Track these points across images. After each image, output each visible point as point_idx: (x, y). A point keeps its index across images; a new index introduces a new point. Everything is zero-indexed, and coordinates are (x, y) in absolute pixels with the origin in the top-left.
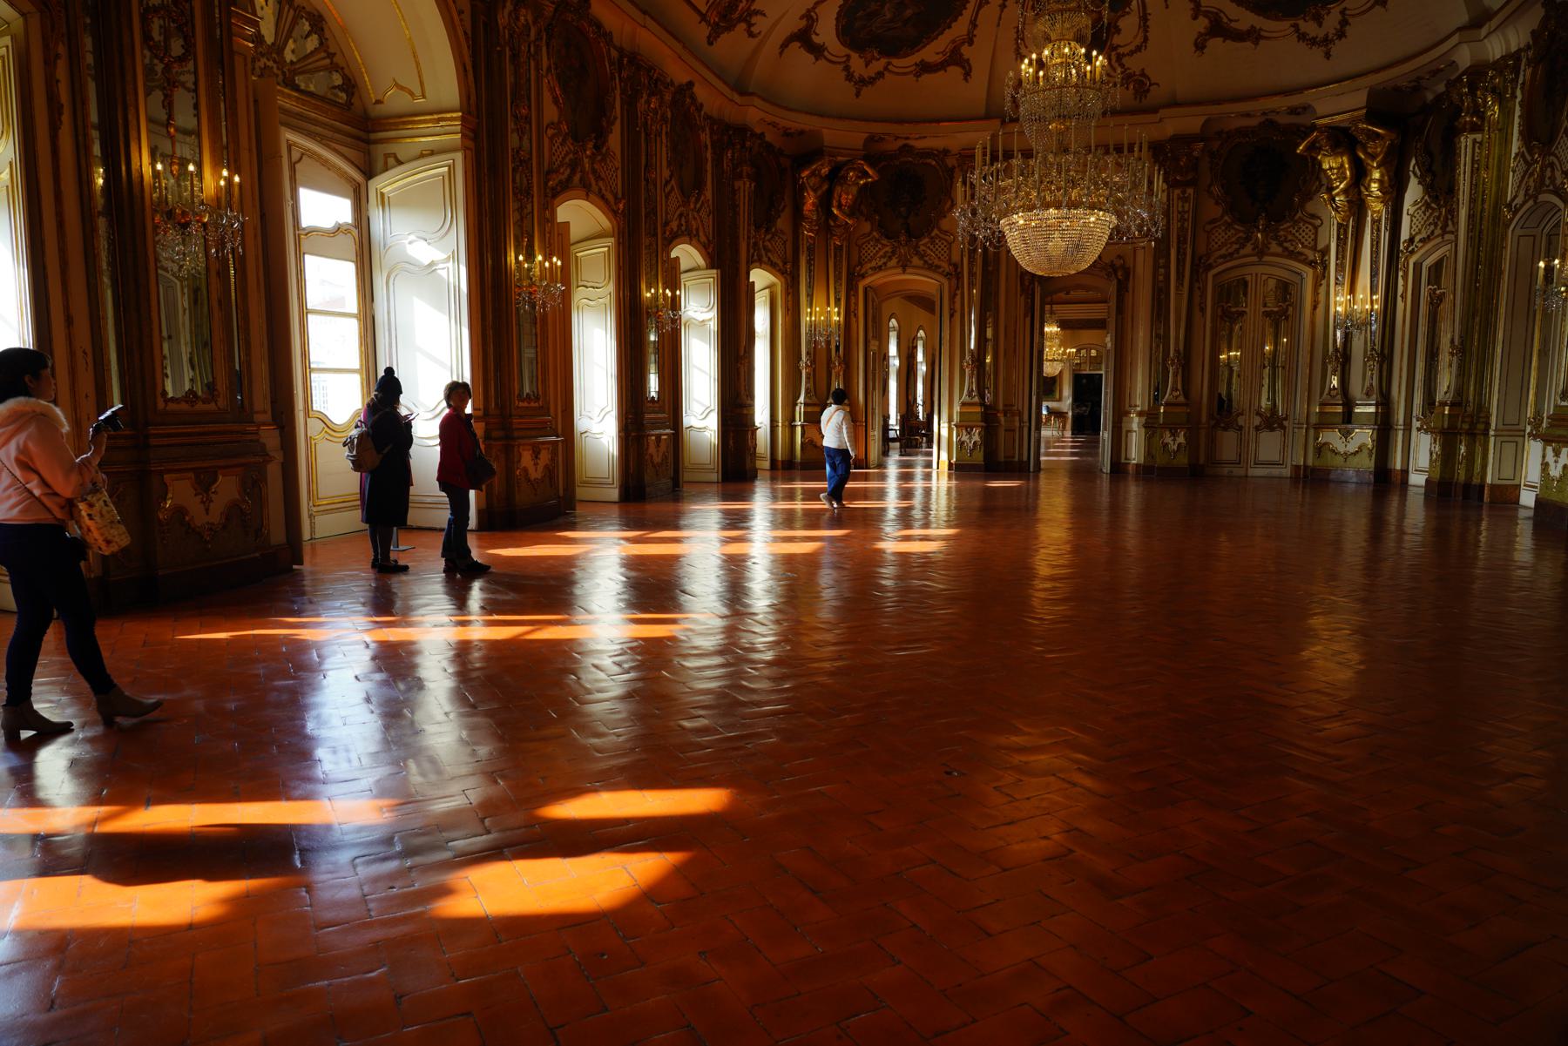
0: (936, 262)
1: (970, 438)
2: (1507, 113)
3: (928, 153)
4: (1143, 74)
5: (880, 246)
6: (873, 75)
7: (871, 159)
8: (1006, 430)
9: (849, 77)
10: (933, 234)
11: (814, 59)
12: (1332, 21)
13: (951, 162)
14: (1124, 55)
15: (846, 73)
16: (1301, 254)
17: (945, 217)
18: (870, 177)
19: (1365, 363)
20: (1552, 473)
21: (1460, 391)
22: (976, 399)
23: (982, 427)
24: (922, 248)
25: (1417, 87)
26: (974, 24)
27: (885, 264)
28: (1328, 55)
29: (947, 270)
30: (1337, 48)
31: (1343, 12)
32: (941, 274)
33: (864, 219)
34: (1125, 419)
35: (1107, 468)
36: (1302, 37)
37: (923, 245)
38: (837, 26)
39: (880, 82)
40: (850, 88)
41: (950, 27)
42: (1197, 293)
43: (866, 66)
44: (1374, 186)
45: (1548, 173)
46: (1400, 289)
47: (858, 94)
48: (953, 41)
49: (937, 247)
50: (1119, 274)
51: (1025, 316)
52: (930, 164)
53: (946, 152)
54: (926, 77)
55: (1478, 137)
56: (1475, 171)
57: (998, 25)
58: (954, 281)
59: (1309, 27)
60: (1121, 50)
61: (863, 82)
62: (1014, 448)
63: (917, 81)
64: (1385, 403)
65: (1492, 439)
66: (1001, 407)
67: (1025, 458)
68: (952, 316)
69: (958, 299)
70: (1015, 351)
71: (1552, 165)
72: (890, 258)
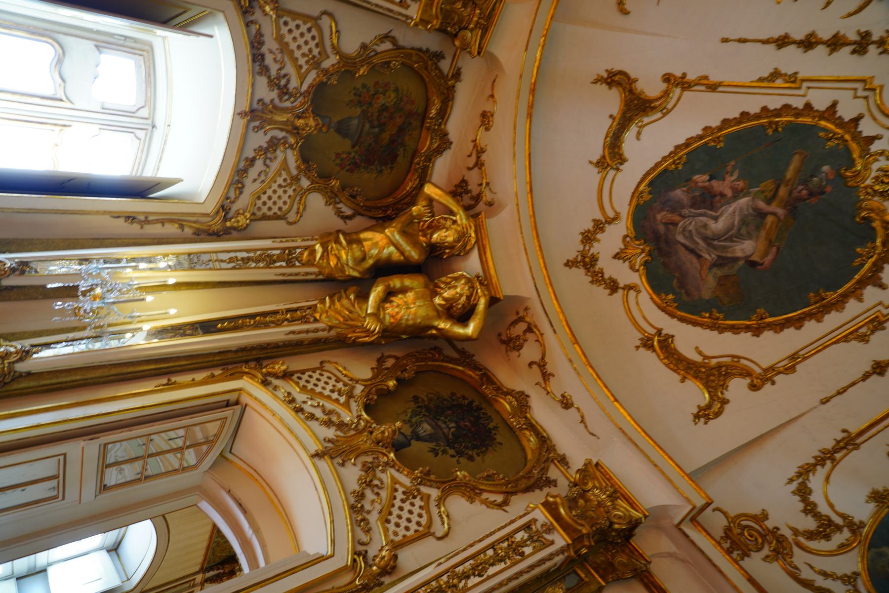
5: (342, 399)
6: (606, 276)
9: (588, 238)
10: (424, 489)
11: (595, 158)
15: (591, 229)
24: (386, 477)
26: (794, 360)
27: (312, 417)
33: (374, 366)
37: (393, 478)
38: (657, 165)
39: (601, 291)
40: (573, 248)
41: (757, 331)
47: (569, 264)
49: (407, 506)
57: (825, 401)
63: (637, 347)
72: (328, 423)
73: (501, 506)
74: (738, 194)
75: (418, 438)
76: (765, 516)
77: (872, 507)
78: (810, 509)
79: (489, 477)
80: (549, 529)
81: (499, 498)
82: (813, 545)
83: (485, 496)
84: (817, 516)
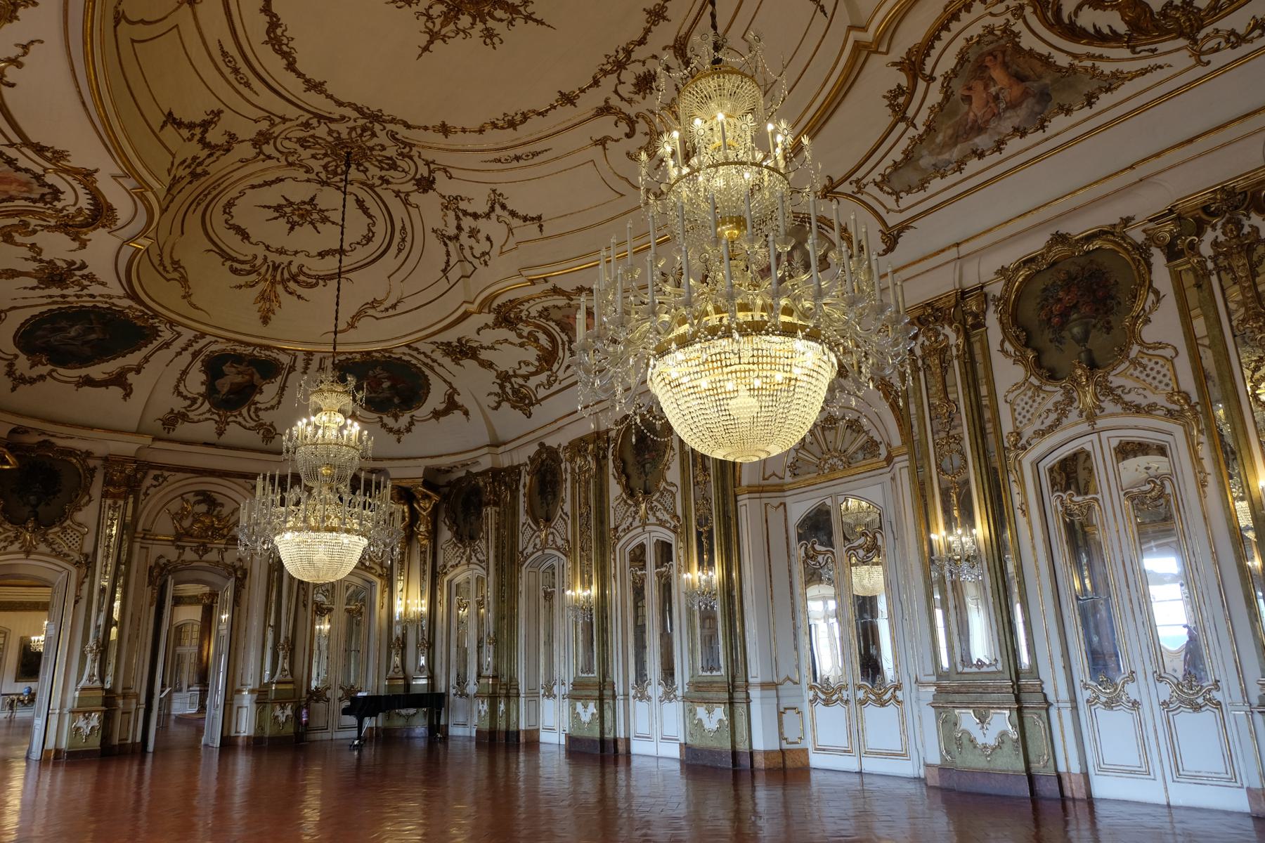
0: (66, 550)
1: (87, 723)
2: (515, 498)
3: (71, 452)
4: (271, 425)
7: (13, 448)
8: (123, 713)
10: (65, 525)
12: (404, 420)
13: (91, 463)
14: (260, 409)
16: (373, 568)
17: (80, 510)
18: (7, 463)
19: (417, 648)
20: (583, 719)
21: (496, 669)
22: (98, 684)
23: (102, 711)
24: (51, 536)
25: (449, 471)
26: (146, 359)
28: (399, 441)
29: (77, 559)
30: (406, 437)
31: (412, 417)
32: (69, 562)
34: (236, 696)
35: (217, 743)
36: (384, 426)
39: (39, 384)
41: (124, 356)
42: (302, 592)
43: (31, 368)
44: (422, 529)
45: (551, 537)
46: (439, 598)
48: (123, 368)
50: (239, 573)
51: (151, 605)
52: (70, 462)
53: (89, 454)
54: (87, 389)
55: (498, 509)
56: (497, 529)
58: (84, 570)
59: (389, 421)
60: (259, 406)
61: (23, 380)
62: (128, 730)
64: (432, 677)
65: (522, 700)
66: (120, 691)
67: (138, 739)
68: (76, 602)
69: (86, 587)
70: (137, 637)
71: (553, 533)
73: (90, 501)
74: (72, 326)
75: (37, 506)
76: (172, 410)
77: (204, 387)
78: (185, 398)
79: (76, 497)
80: (115, 503)
81: (87, 498)
82: (193, 408)
83: (82, 503)
84: (189, 399)
